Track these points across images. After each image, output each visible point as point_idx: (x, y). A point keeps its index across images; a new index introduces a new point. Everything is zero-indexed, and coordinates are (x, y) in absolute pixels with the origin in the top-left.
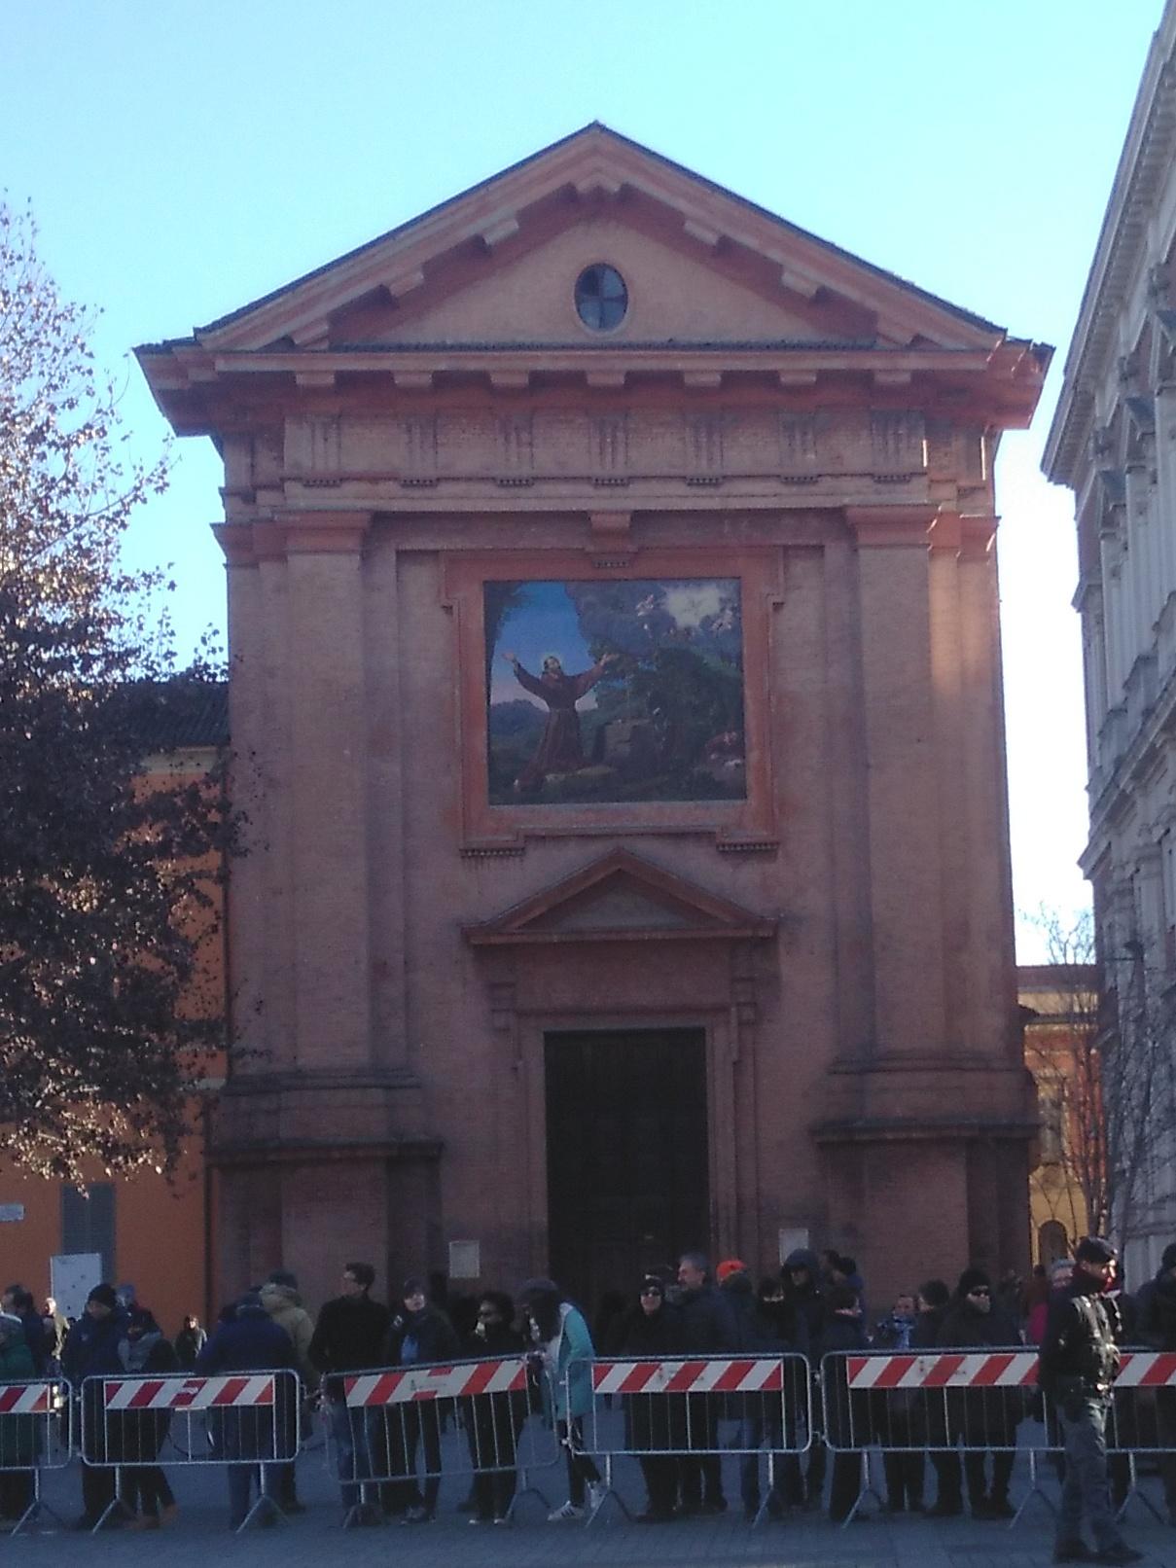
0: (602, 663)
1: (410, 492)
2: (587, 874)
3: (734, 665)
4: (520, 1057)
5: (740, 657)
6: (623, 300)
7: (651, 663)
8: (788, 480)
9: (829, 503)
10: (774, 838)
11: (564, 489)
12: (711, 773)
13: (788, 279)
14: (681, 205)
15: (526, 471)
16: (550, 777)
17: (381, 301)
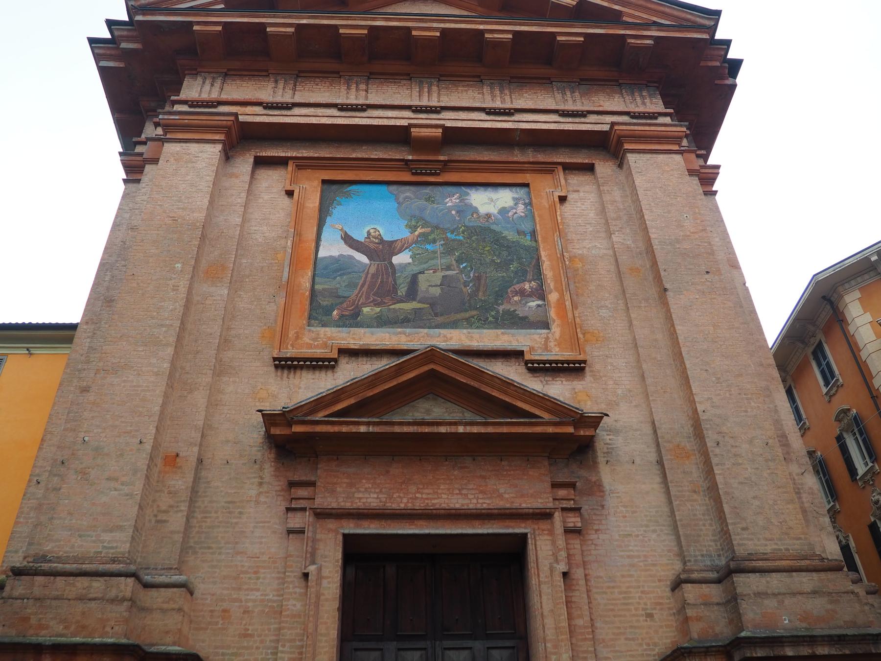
0: (417, 233)
3: (528, 238)
4: (313, 562)
5: (533, 234)
7: (458, 235)
12: (515, 311)
16: (366, 310)
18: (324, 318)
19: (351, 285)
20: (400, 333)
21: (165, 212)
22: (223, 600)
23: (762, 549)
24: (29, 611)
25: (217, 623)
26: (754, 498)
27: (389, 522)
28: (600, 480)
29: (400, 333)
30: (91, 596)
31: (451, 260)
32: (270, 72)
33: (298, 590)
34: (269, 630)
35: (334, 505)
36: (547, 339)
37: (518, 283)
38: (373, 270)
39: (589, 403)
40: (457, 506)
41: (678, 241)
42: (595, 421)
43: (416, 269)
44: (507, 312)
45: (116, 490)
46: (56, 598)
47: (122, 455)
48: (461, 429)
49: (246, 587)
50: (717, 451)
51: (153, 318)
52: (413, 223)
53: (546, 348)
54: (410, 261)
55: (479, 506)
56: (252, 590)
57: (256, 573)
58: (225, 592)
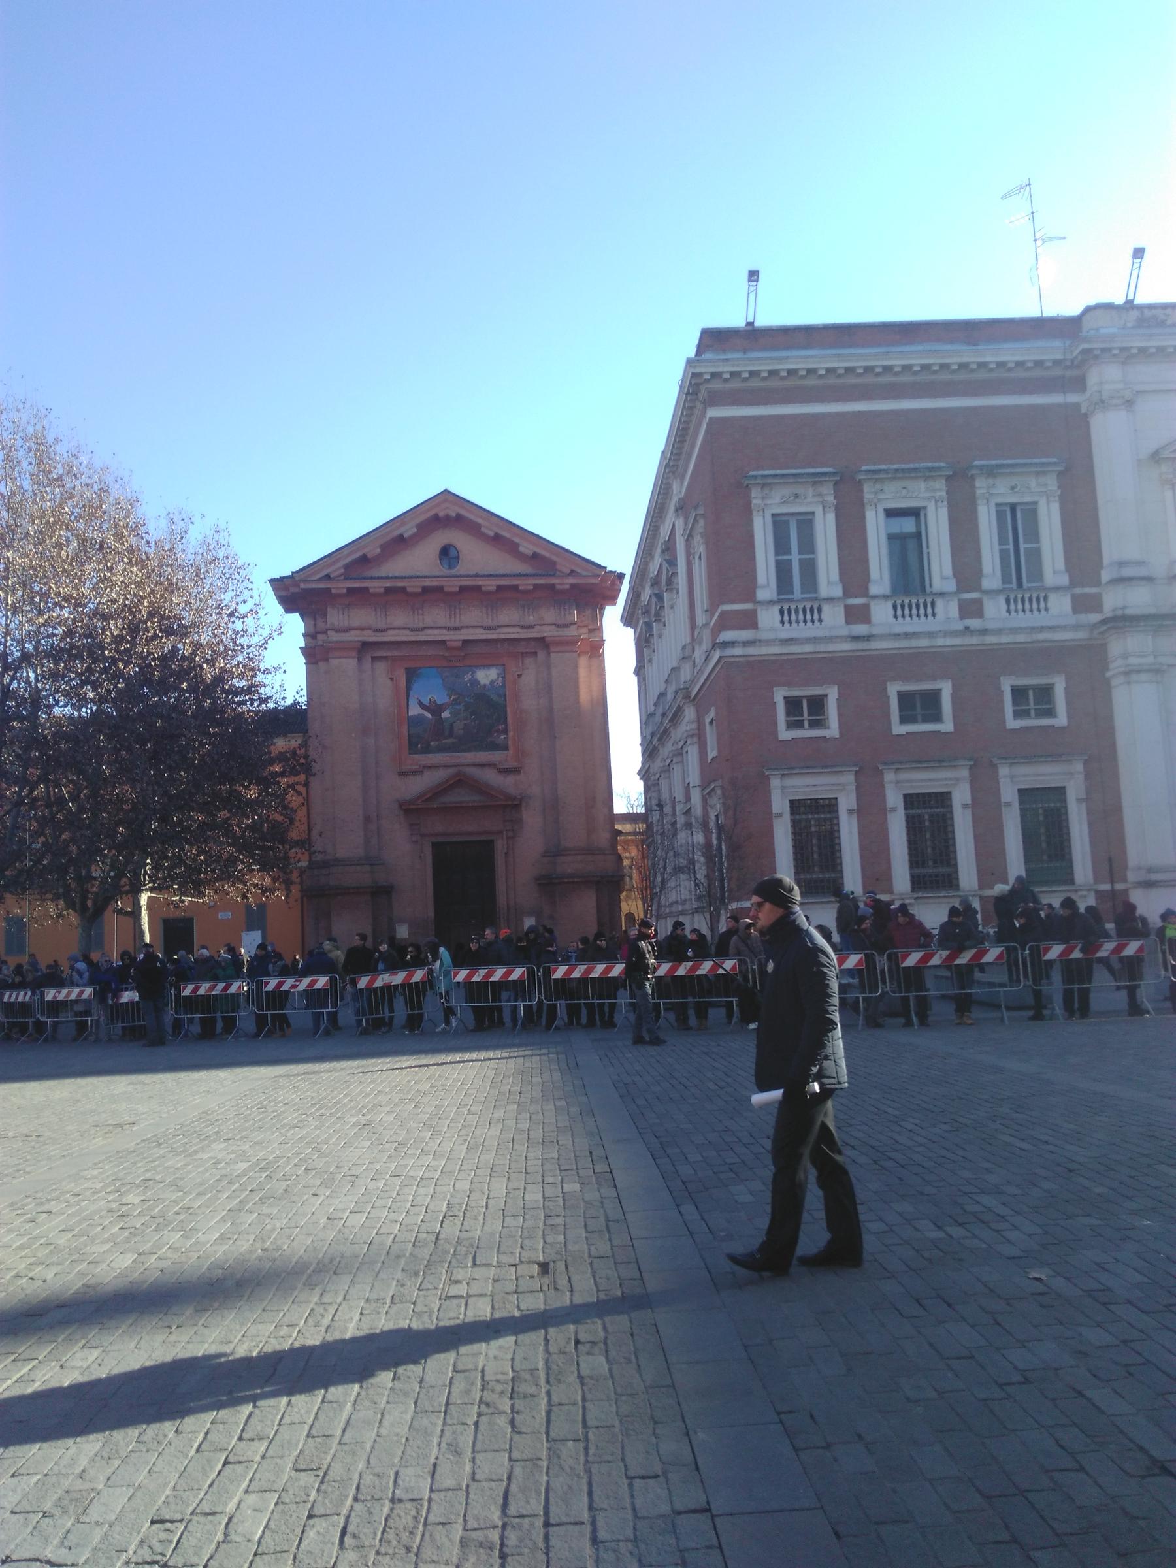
1: (376, 634)
2: (447, 781)
5: (505, 695)
6: (458, 558)
8: (523, 627)
9: (539, 635)
11: (436, 632)
13: (521, 549)
14: (480, 521)
15: (421, 625)
16: (432, 743)
17: (364, 560)
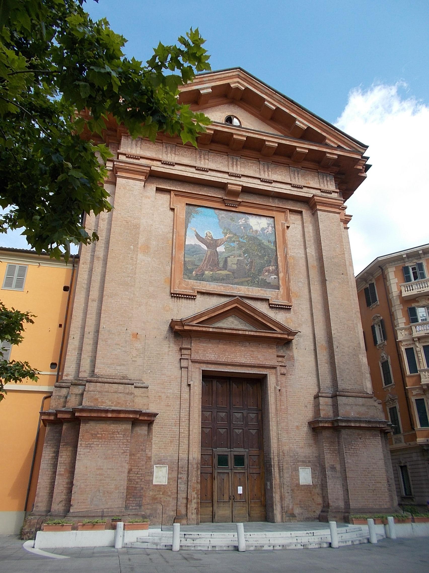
0: (227, 237)
3: (273, 245)
7: (244, 239)
10: (290, 304)
16: (206, 272)
18: (190, 275)
19: (200, 260)
20: (221, 286)
21: (122, 217)
22: (158, 392)
23: (347, 388)
24: (97, 396)
25: (157, 401)
26: (347, 369)
27: (218, 366)
28: (293, 355)
29: (221, 286)
30: (119, 391)
31: (241, 252)
32: (163, 141)
33: (186, 390)
34: (176, 404)
35: (198, 358)
36: (278, 294)
37: (267, 266)
38: (209, 253)
39: (292, 323)
40: (243, 362)
41: (333, 258)
42: (294, 334)
43: (226, 255)
44: (262, 279)
45: (119, 349)
46: (106, 392)
47: (120, 334)
48: (247, 333)
49: (166, 388)
50: (337, 350)
51: (124, 272)
52: (225, 231)
53: (277, 298)
54: (224, 250)
55: (251, 362)
56: (169, 389)
57: (170, 382)
58: (159, 389)
